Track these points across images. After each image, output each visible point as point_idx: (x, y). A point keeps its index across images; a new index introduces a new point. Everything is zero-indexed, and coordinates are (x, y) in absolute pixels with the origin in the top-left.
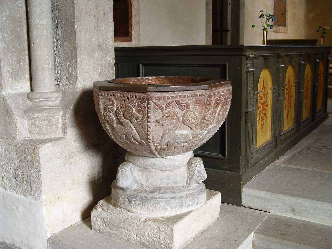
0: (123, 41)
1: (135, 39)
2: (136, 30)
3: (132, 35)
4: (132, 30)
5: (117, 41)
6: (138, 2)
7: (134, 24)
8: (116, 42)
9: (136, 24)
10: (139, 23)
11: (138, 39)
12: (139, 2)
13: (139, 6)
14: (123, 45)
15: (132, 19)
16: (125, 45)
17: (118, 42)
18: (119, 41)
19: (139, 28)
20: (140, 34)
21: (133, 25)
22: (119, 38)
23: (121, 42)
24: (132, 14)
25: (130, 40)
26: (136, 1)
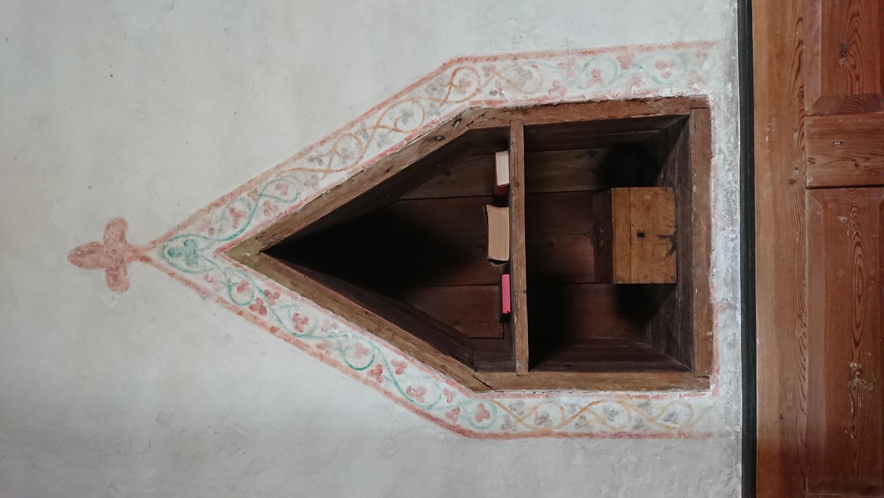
0: (707, 156)
1: (700, 80)
2: (658, 73)
3: (680, 100)
4: (657, 100)
5: (708, 200)
6: (540, 61)
7: (634, 88)
8: (712, 204)
9: (632, 70)
10: (623, 48)
11: (698, 55)
12: (538, 55)
13: (551, 55)
14: (725, 159)
15: (610, 98)
16: (724, 148)
17: (713, 195)
18: (707, 188)
19: (649, 48)
20: (676, 46)
21: (635, 92)
22: (694, 188)
23: (712, 174)
24: (590, 102)
25: (701, 106)
26: (533, 70)
